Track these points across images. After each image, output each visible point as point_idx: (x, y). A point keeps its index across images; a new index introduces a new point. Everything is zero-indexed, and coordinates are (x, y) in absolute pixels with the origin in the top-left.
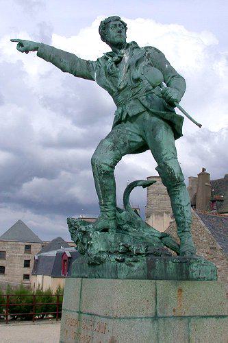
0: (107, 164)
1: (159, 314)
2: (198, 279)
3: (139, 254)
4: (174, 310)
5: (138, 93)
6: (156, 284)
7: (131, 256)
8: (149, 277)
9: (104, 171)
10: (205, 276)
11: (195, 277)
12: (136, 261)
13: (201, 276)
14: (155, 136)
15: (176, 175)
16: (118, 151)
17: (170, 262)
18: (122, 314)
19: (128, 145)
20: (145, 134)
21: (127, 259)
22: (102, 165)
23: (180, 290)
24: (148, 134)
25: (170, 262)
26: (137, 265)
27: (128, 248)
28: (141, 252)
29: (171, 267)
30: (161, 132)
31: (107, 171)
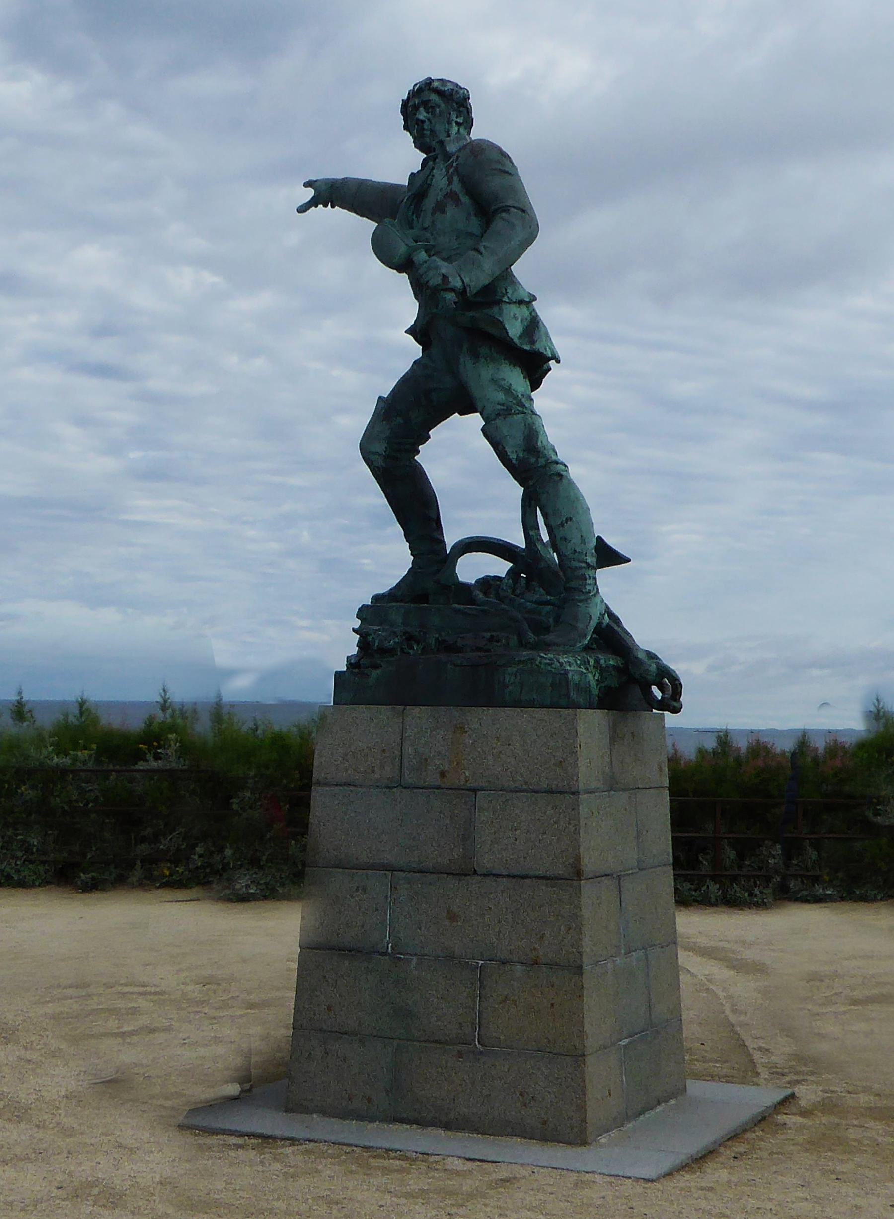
0: (377, 453)
2: (516, 704)
4: (443, 774)
16: (400, 420)
18: (329, 776)
22: (373, 457)
25: (449, 667)
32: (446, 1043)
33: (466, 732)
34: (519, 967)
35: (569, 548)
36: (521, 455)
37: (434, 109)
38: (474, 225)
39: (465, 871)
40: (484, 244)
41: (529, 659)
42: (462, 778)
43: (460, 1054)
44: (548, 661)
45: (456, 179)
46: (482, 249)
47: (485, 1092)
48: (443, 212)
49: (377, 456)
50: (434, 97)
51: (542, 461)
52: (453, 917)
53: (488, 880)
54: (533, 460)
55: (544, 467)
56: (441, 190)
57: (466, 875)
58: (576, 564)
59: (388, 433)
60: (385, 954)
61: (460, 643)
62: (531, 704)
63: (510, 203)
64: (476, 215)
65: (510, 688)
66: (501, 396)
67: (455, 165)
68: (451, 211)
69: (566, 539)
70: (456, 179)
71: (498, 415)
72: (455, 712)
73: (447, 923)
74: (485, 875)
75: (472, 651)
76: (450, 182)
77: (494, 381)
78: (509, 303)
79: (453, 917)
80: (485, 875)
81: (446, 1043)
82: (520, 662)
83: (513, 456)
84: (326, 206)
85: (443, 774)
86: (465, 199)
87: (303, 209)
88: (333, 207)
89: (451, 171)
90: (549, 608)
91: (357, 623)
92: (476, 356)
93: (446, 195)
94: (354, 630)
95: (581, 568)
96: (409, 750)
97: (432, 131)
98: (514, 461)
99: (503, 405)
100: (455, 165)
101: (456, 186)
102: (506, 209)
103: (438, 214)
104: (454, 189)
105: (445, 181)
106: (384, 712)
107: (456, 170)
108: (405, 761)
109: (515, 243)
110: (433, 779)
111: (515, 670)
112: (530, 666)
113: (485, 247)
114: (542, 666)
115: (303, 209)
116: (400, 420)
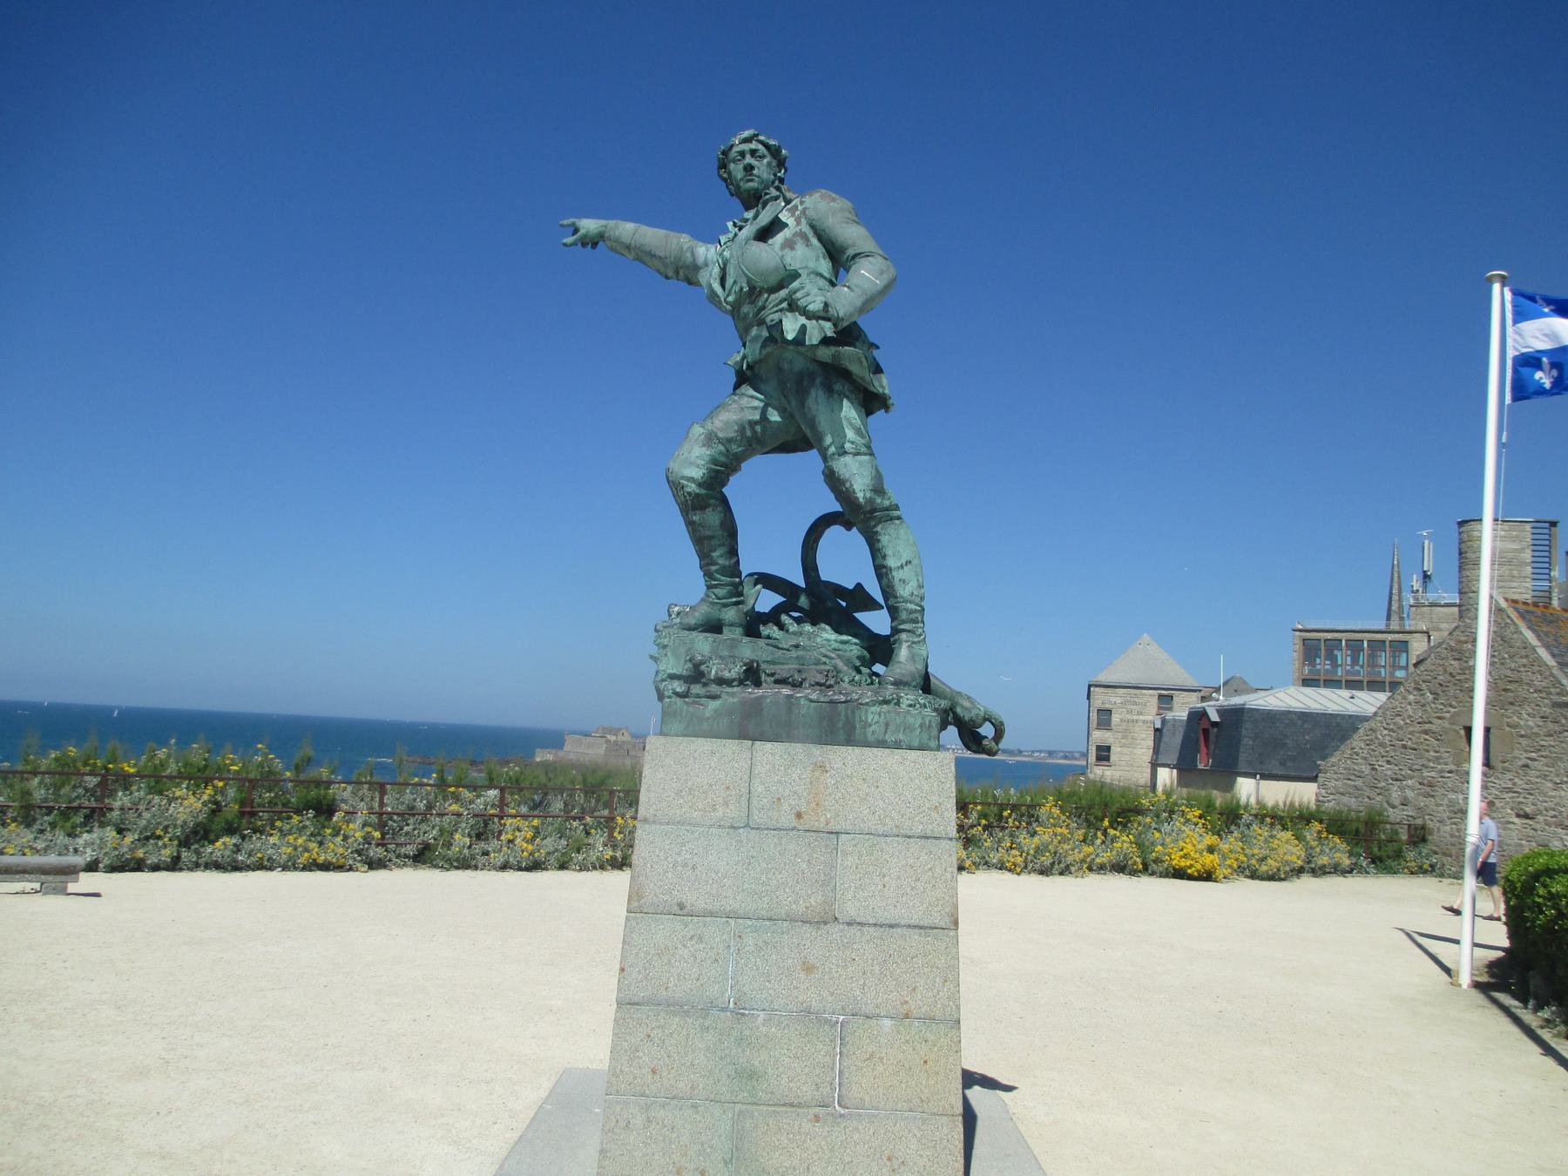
0: (691, 479)
1: (757, 817)
2: (881, 744)
3: (721, 681)
4: (799, 815)
5: (764, 308)
7: (705, 685)
8: (743, 735)
10: (901, 737)
11: (871, 738)
12: (714, 697)
13: (890, 737)
15: (860, 495)
17: (802, 702)
18: (659, 813)
21: (696, 689)
24: (793, 403)
25: (802, 702)
27: (697, 666)
28: (727, 675)
29: (803, 711)
30: (813, 393)
31: (698, 495)
32: (799, 1106)
34: (887, 1023)
38: (825, 266)
39: (825, 920)
42: (822, 820)
43: (817, 1118)
47: (847, 1159)
48: (792, 249)
50: (760, 147)
52: (809, 969)
53: (853, 930)
54: (879, 501)
57: (826, 923)
60: (724, 1010)
62: (897, 745)
70: (803, 221)
72: (817, 751)
73: (802, 975)
74: (849, 924)
79: (809, 969)
80: (849, 924)
81: (799, 1106)
85: (799, 815)
86: (815, 241)
92: (829, 390)
96: (758, 788)
106: (731, 746)
108: (754, 802)
110: (787, 819)
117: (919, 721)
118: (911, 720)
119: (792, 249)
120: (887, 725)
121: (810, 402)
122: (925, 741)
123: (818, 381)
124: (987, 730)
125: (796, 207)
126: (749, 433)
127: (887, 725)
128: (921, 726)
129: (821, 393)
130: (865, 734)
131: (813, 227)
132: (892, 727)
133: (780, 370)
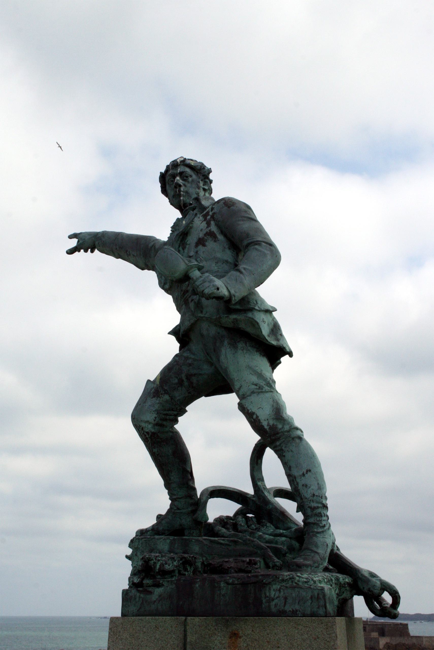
0: (147, 422)
2: (282, 613)
6: (185, 624)
7: (153, 577)
9: (148, 433)
10: (297, 607)
11: (274, 610)
12: (158, 585)
13: (288, 608)
14: (219, 360)
19: (186, 383)
20: (211, 357)
22: (143, 425)
23: (235, 635)
25: (222, 584)
26: (158, 591)
29: (223, 592)
30: (223, 351)
31: (153, 434)
33: (240, 637)
35: (309, 492)
36: (271, 423)
37: (183, 181)
38: (228, 255)
40: (245, 266)
41: (290, 578)
44: (305, 580)
45: (212, 223)
46: (243, 270)
49: (147, 424)
50: (188, 170)
51: (287, 428)
54: (280, 426)
55: (288, 431)
56: (202, 230)
58: (314, 505)
59: (157, 407)
61: (227, 565)
62: (294, 613)
63: (259, 239)
64: (229, 249)
65: (276, 601)
66: (254, 379)
67: (211, 213)
68: (210, 244)
69: (306, 486)
70: (212, 223)
71: (253, 392)
75: (236, 572)
76: (209, 224)
77: (249, 367)
78: (259, 311)
82: (283, 580)
83: (265, 424)
84: (86, 251)
86: (220, 237)
87: (71, 252)
88: (92, 252)
89: (209, 217)
90: (284, 539)
91: (129, 551)
93: (207, 234)
94: (127, 557)
95: (318, 508)
97: (187, 192)
98: (266, 427)
99: (256, 385)
100: (211, 213)
101: (213, 228)
102: (258, 243)
103: (200, 247)
104: (212, 230)
105: (204, 224)
107: (212, 217)
109: (265, 267)
111: (279, 587)
112: (290, 583)
113: (245, 269)
114: (300, 584)
115: (71, 252)
116: (167, 397)
117: (310, 594)
118: (304, 594)
119: (204, 245)
120: (286, 598)
121: (222, 358)
122: (315, 609)
123: (226, 343)
124: (387, 597)
125: (208, 213)
126: (186, 383)
127: (286, 598)
128: (311, 598)
129: (228, 350)
130: (269, 606)
131: (217, 225)
132: (290, 601)
133: (202, 335)
